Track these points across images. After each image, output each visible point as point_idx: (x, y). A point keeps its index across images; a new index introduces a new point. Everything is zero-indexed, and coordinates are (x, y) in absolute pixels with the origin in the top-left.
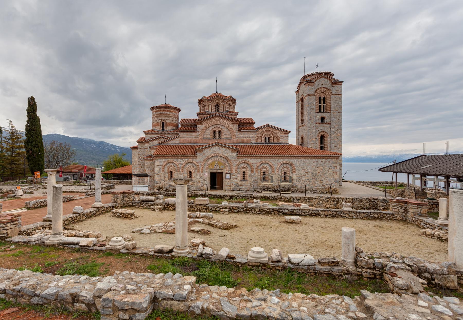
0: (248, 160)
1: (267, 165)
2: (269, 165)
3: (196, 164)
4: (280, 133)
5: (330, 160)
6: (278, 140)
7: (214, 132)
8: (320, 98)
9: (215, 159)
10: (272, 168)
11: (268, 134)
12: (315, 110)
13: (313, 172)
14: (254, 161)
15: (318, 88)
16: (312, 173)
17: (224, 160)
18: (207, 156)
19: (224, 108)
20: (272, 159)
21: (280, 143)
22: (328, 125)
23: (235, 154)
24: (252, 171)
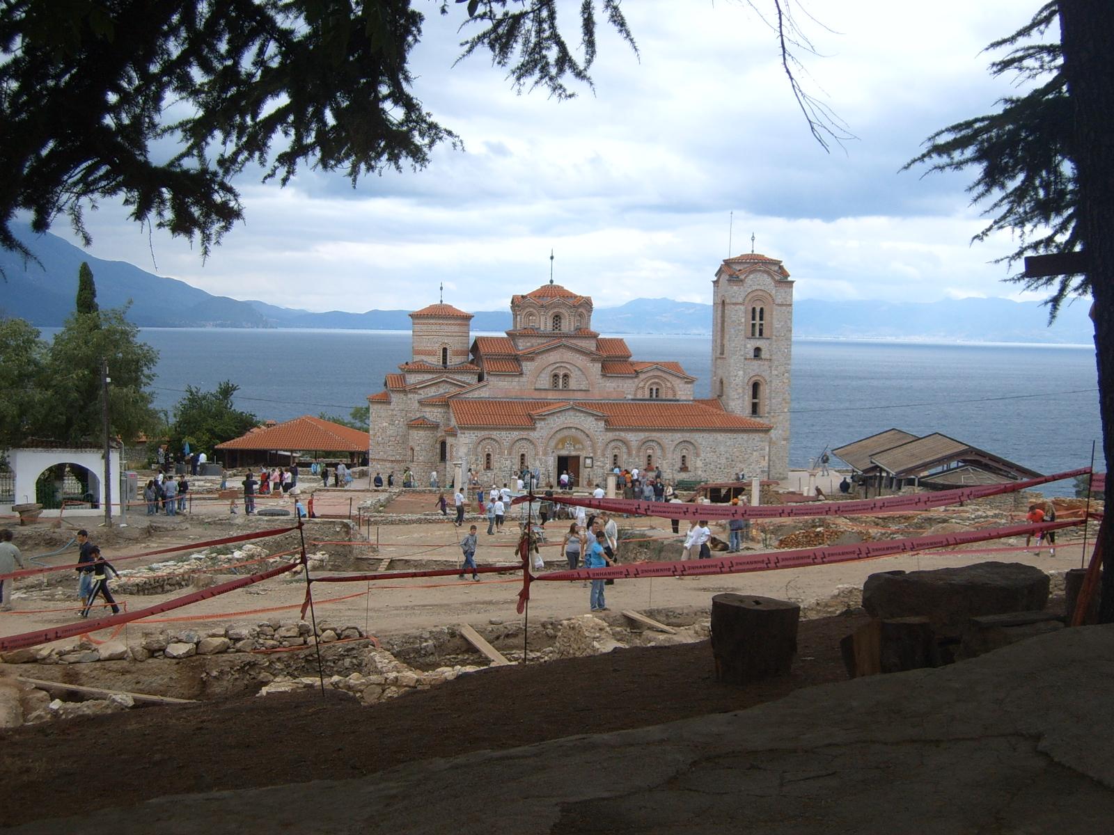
0: (623, 434)
1: (654, 444)
2: (659, 444)
3: (534, 440)
4: (678, 381)
5: (757, 436)
6: (675, 395)
7: (556, 376)
8: (754, 309)
9: (566, 433)
10: (662, 448)
11: (657, 383)
12: (743, 332)
13: (728, 455)
14: (633, 438)
15: (750, 290)
16: (727, 458)
17: (580, 436)
18: (552, 428)
19: (567, 325)
20: (662, 434)
21: (678, 400)
22: (766, 363)
23: (602, 424)
24: (629, 454)
